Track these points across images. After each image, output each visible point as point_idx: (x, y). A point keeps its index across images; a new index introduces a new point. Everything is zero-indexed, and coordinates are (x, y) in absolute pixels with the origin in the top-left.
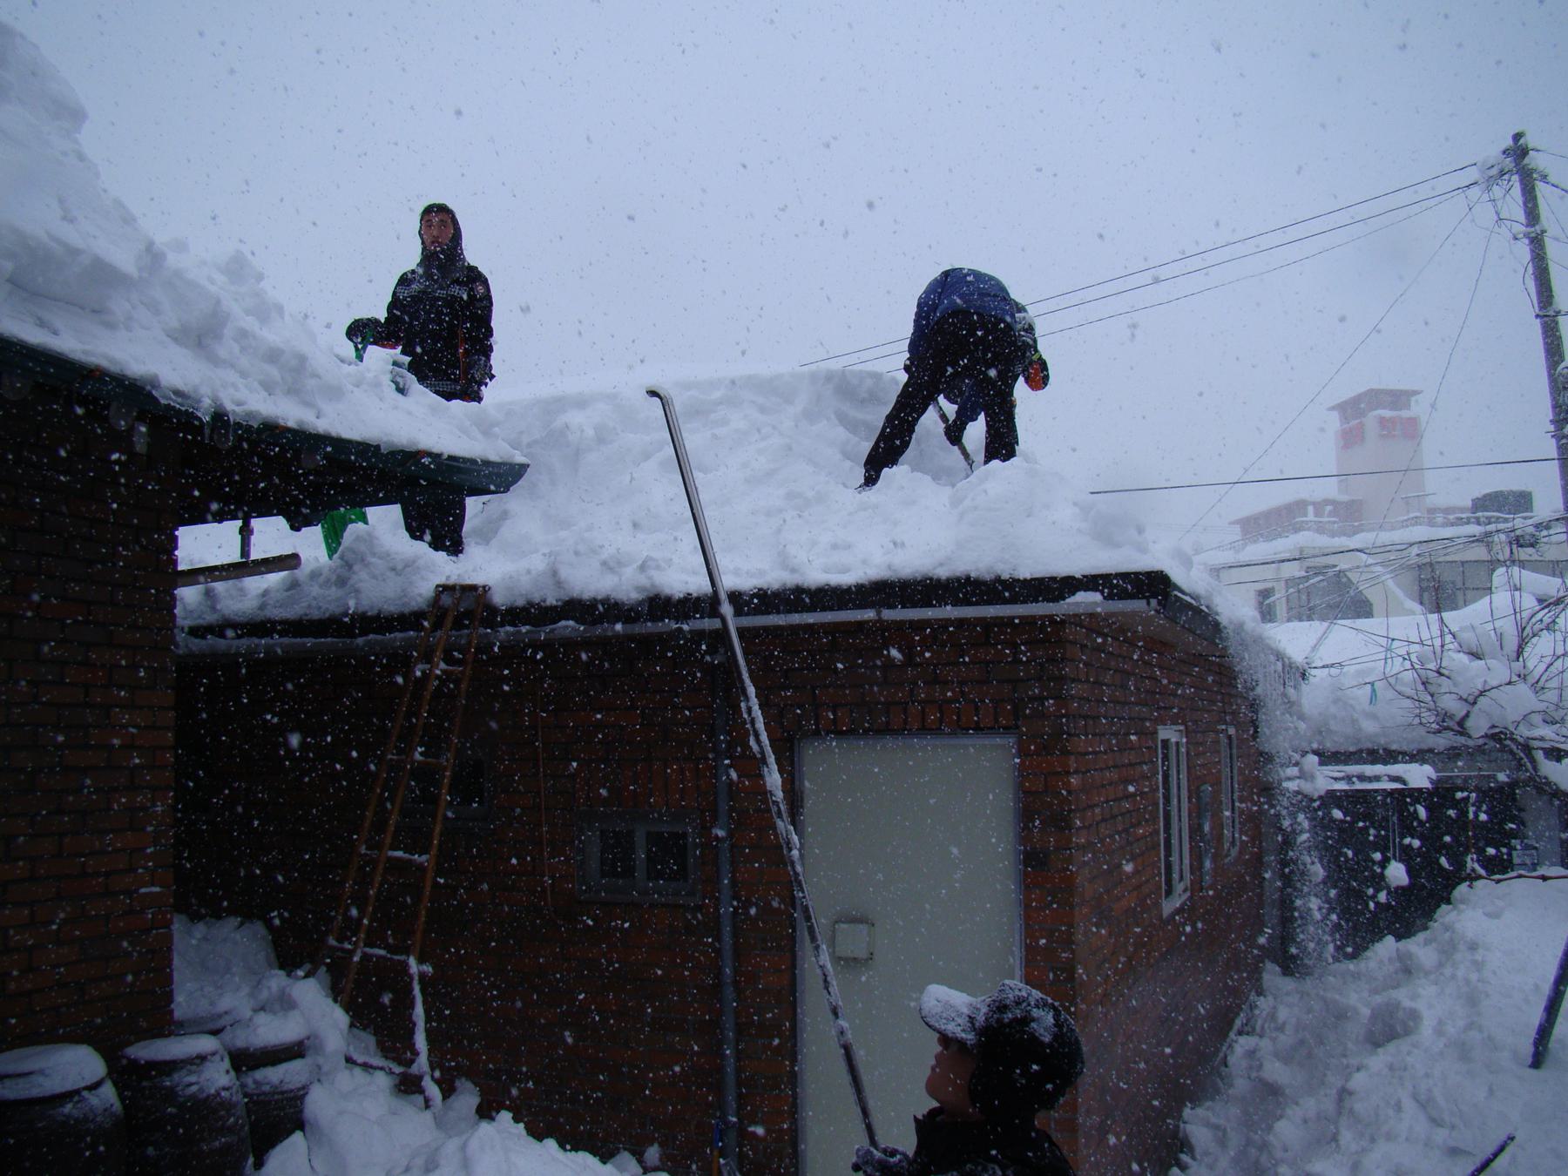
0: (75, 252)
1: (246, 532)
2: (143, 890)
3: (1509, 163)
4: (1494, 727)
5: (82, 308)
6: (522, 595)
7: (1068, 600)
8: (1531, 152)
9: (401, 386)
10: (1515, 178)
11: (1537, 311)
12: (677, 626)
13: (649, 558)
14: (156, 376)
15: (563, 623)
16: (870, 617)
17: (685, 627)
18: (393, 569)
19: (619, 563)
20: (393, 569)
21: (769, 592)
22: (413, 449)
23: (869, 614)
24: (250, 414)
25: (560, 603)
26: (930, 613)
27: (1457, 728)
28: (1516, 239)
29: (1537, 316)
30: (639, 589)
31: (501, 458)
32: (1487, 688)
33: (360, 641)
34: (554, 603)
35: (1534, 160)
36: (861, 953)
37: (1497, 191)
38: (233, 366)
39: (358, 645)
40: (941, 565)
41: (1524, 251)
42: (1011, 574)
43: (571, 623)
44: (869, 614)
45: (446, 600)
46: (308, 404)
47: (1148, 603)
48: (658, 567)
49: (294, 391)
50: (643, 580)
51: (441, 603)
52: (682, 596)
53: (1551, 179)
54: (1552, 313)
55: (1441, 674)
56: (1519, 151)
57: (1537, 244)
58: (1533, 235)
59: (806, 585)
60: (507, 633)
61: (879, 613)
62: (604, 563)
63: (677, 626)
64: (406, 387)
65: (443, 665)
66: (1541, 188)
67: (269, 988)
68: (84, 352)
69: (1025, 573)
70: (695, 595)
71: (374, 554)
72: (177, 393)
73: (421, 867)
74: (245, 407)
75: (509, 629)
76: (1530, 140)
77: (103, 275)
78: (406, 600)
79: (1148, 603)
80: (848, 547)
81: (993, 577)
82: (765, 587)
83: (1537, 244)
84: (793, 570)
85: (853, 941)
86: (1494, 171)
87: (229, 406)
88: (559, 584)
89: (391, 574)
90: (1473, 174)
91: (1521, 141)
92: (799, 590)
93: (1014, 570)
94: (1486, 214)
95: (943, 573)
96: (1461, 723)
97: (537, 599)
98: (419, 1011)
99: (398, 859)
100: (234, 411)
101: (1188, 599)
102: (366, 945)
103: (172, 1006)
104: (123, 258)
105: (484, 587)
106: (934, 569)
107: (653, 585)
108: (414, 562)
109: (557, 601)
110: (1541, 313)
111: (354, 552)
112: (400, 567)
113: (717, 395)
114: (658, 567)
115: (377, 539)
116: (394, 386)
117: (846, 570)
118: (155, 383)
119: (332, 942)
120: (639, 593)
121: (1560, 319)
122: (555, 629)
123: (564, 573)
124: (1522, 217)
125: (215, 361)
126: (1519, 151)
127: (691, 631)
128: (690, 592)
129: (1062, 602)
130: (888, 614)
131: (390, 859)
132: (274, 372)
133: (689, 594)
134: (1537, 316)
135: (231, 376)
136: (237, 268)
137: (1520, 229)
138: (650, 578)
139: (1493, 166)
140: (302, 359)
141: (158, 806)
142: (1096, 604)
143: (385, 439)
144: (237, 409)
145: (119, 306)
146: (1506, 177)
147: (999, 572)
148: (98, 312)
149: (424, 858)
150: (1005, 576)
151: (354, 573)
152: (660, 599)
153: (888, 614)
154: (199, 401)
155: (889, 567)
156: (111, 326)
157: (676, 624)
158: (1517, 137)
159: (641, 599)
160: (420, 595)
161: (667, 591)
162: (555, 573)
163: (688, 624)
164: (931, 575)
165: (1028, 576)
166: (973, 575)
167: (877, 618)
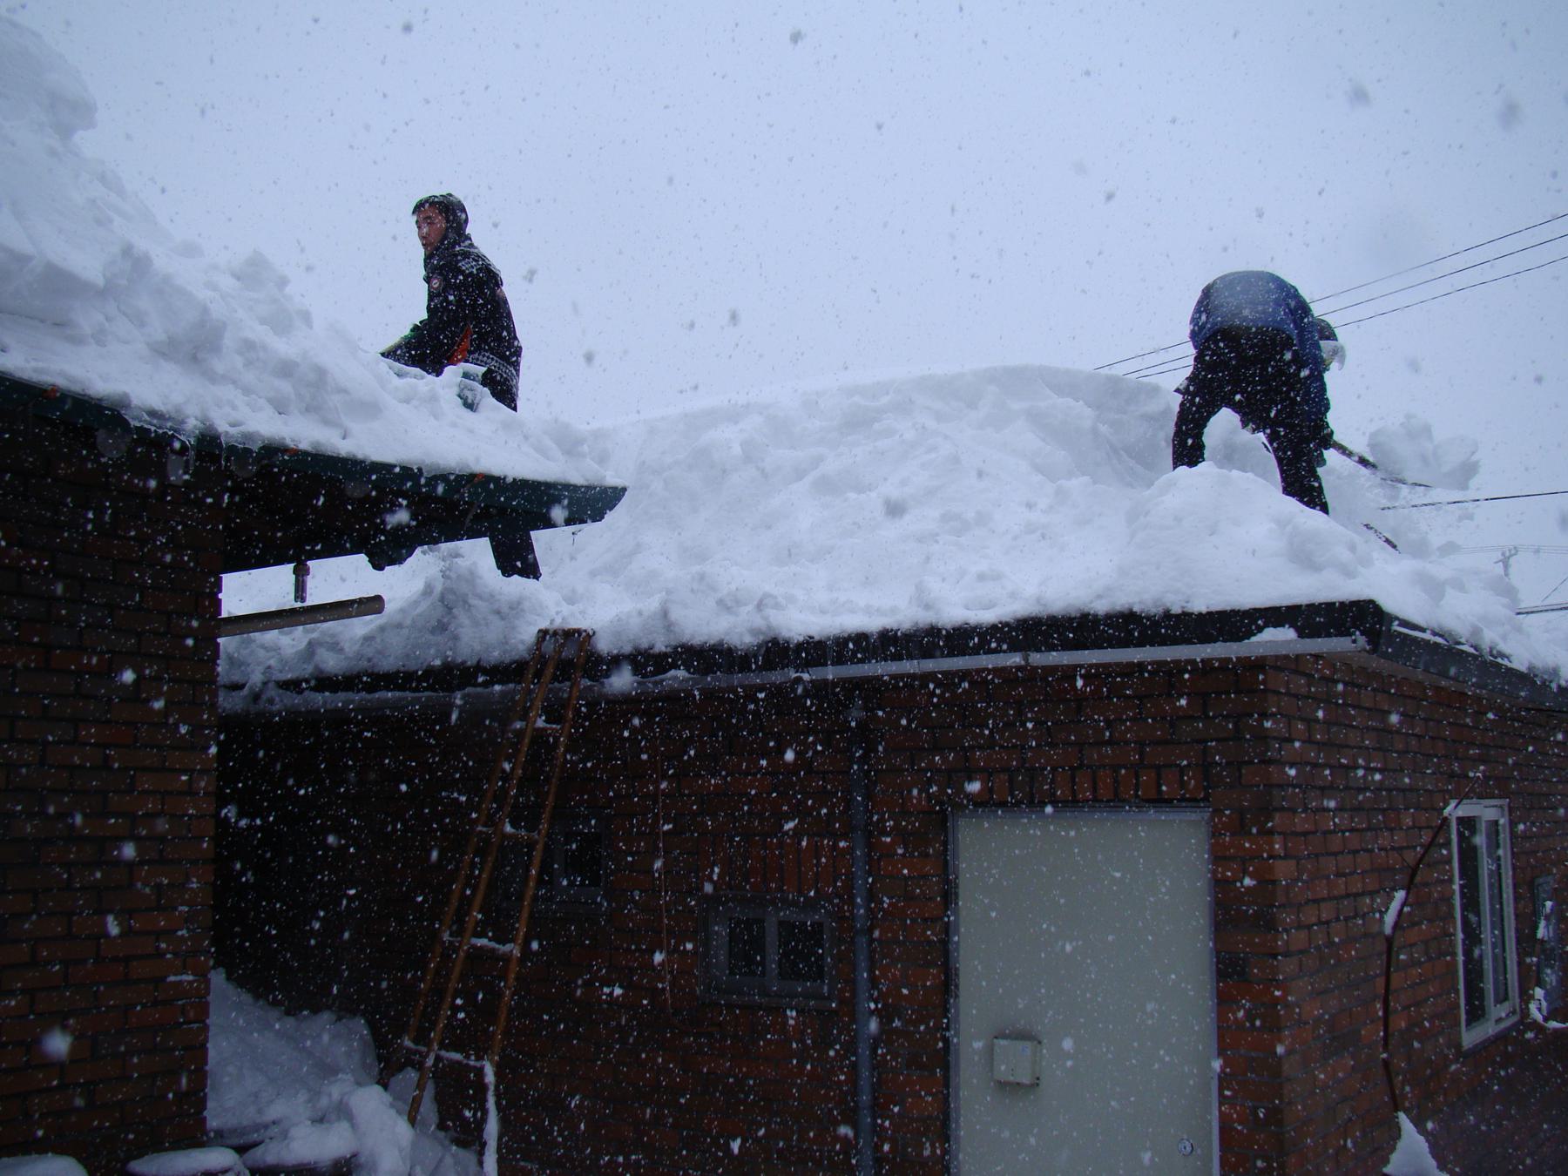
0: (22, 259)
1: (301, 573)
2: (172, 978)
5: (42, 321)
7: (1254, 639)
9: (470, 401)
12: (798, 674)
13: (767, 595)
14: (126, 395)
15: (673, 673)
17: (806, 677)
18: (498, 613)
19: (738, 603)
20: (498, 613)
21: (899, 634)
22: (466, 472)
24: (248, 436)
25: (669, 650)
30: (754, 632)
31: (587, 480)
34: (664, 649)
36: (1026, 1080)
38: (234, 382)
40: (1099, 597)
42: (1183, 607)
46: (326, 422)
48: (777, 606)
49: (313, 408)
50: (759, 622)
52: (801, 639)
61: (1026, 659)
62: (720, 602)
63: (798, 674)
64: (476, 402)
67: (330, 1095)
68: (35, 370)
69: (1199, 606)
70: (817, 638)
71: (480, 597)
72: (153, 413)
73: (507, 958)
74: (241, 428)
77: (60, 283)
80: (997, 577)
81: (1161, 610)
82: (895, 628)
84: (927, 607)
85: (1013, 1062)
87: (222, 427)
88: (669, 627)
89: (494, 618)
92: (933, 631)
93: (1187, 602)
95: (1101, 607)
97: (644, 645)
98: (492, 1128)
99: (481, 948)
100: (227, 433)
101: (1427, 636)
102: (442, 1046)
103: (205, 1113)
104: (87, 263)
106: (1091, 602)
107: (769, 627)
108: (519, 603)
109: (666, 647)
111: (455, 593)
112: (505, 609)
113: (885, 400)
114: (777, 606)
115: (481, 578)
116: (460, 401)
117: (990, 606)
118: (127, 406)
119: (408, 1043)
123: (676, 614)
125: (213, 378)
127: (812, 681)
128: (812, 634)
129: (1247, 641)
130: (1037, 659)
131: (474, 947)
132: (286, 387)
133: (811, 637)
135: (228, 392)
136: (253, 272)
138: (766, 619)
140: (321, 373)
141: (193, 883)
143: (428, 461)
144: (232, 431)
145: (87, 318)
147: (1168, 605)
148: (61, 326)
149: (508, 947)
150: (1176, 610)
151: (455, 617)
152: (778, 643)
153: (1037, 659)
154: (183, 422)
155: (1038, 600)
156: (77, 340)
157: (797, 672)
160: (522, 642)
162: (665, 614)
163: (808, 673)
164: (1086, 610)
165: (1204, 610)
166: (1136, 609)
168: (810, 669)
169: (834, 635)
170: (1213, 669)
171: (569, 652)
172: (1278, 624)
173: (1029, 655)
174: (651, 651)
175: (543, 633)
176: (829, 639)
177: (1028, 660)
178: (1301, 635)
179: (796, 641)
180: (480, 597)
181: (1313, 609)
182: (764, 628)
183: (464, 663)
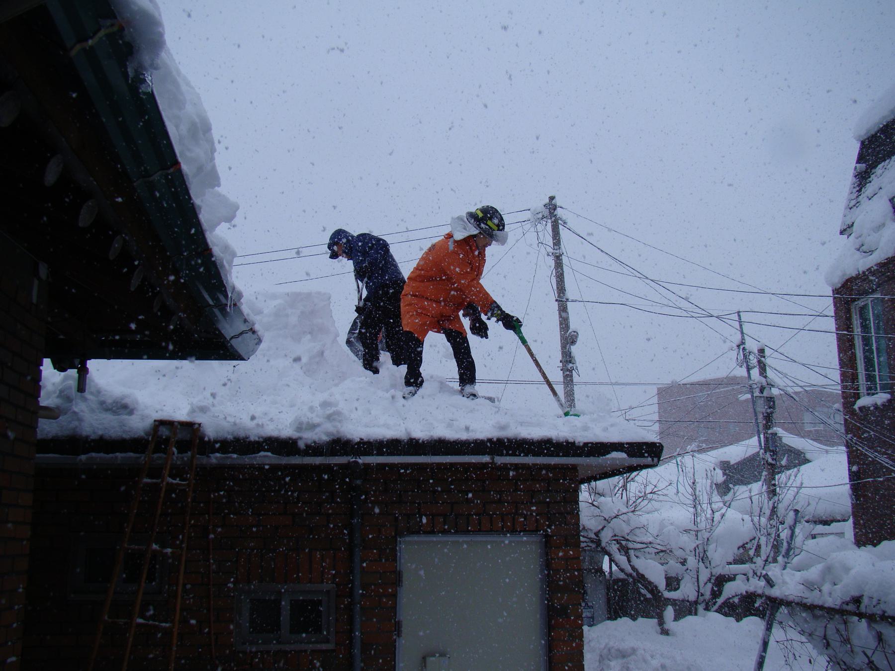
3: (546, 212)
4: (615, 536)
6: (228, 433)
7: (607, 456)
8: (558, 209)
10: (550, 221)
11: (557, 297)
15: (262, 453)
16: (487, 460)
17: (360, 461)
23: (486, 459)
25: (261, 440)
26: (467, 459)
27: (593, 536)
28: (548, 255)
29: (556, 300)
30: (327, 434)
32: (620, 513)
33: (83, 457)
34: (257, 439)
35: (559, 212)
37: (539, 227)
39: (81, 460)
41: (551, 262)
43: (269, 454)
44: (486, 459)
45: (164, 432)
47: (653, 460)
51: (160, 433)
53: (569, 225)
54: (564, 300)
55: (593, 505)
56: (552, 206)
57: (558, 259)
58: (558, 254)
59: (447, 439)
60: (216, 458)
61: (493, 459)
63: (354, 459)
65: (170, 480)
66: (563, 231)
70: (365, 440)
75: (218, 455)
76: (558, 201)
78: (127, 429)
79: (653, 460)
83: (558, 259)
86: (540, 216)
90: (527, 215)
91: (553, 202)
94: (531, 237)
96: (597, 534)
97: (242, 434)
105: (200, 424)
107: (338, 432)
109: (259, 438)
110: (558, 299)
120: (328, 436)
121: (569, 304)
122: (256, 457)
124: (551, 244)
126: (552, 206)
127: (364, 464)
128: (363, 437)
134: (556, 300)
137: (550, 250)
139: (540, 213)
142: (623, 459)
146: (545, 219)
157: (352, 458)
158: (552, 198)
159: (328, 440)
161: (349, 436)
167: (491, 461)
168: (361, 457)
169: (380, 440)
170: (568, 468)
171: (181, 435)
172: (617, 450)
173: (494, 457)
174: (248, 440)
175: (161, 423)
176: (376, 441)
177: (494, 459)
178: (628, 455)
179: (356, 441)
180: (92, 393)
181: (631, 444)
182: (335, 432)
183: (87, 437)
